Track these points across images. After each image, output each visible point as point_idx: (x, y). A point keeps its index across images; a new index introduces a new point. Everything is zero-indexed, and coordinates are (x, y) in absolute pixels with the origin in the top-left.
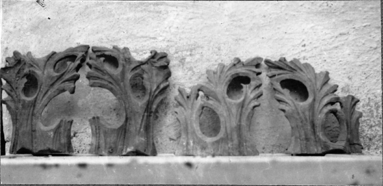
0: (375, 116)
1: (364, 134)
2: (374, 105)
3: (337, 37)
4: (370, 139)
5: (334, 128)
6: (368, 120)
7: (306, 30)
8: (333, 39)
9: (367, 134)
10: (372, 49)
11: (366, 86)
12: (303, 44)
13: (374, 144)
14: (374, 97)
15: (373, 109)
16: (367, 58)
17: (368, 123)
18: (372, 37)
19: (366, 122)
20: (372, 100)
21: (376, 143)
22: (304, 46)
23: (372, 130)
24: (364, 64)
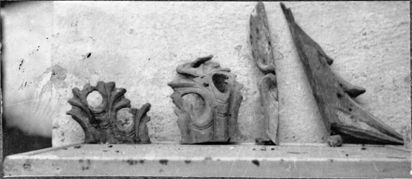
3: (399, 26)
5: (397, 119)
7: (366, 19)
8: (395, 28)
12: (364, 32)
22: (365, 34)
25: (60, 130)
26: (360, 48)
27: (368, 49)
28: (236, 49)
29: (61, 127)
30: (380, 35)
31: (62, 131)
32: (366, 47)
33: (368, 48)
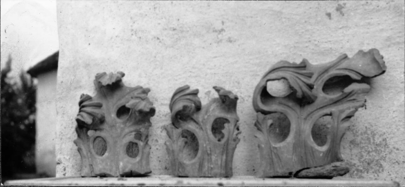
0: (371, 143)
11: (363, 117)
13: (372, 168)
15: (370, 136)
19: (365, 148)
20: (369, 128)
21: (374, 167)
23: (370, 156)
25: (62, 165)
28: (206, 94)
29: (63, 163)
31: (64, 166)
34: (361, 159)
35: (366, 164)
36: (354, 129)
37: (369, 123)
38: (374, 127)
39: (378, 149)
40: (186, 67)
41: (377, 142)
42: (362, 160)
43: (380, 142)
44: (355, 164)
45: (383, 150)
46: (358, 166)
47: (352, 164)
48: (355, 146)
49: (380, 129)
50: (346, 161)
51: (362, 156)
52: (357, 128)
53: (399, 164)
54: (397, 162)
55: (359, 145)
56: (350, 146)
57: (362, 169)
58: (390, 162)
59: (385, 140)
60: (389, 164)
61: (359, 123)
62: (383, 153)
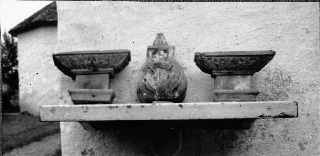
0: (280, 80)
1: (274, 91)
2: (279, 72)
3: (256, 31)
4: (278, 94)
6: (276, 82)
8: (254, 32)
9: (276, 91)
10: (277, 38)
12: (236, 35)
13: (280, 97)
14: (279, 68)
15: (279, 75)
16: (274, 43)
17: (276, 84)
18: (277, 30)
19: (276, 83)
21: (282, 96)
22: (237, 36)
24: (272, 47)
26: (234, 44)
27: (238, 45)
30: (245, 37)
31: (65, 100)
32: (237, 44)
33: (239, 44)
34: (273, 91)
35: (277, 94)
36: (268, 70)
37: (279, 65)
38: (283, 68)
39: (285, 83)
40: (149, 28)
41: (284, 79)
42: (273, 91)
43: (287, 78)
44: (269, 95)
45: (288, 84)
46: (271, 96)
47: (267, 95)
48: (268, 82)
49: (287, 70)
50: (262, 93)
51: (274, 89)
52: (270, 69)
53: (299, 94)
54: (298, 92)
55: (272, 81)
56: (265, 82)
57: (273, 98)
58: (293, 93)
59: (290, 77)
60: (292, 94)
61: (271, 65)
62: (288, 86)
